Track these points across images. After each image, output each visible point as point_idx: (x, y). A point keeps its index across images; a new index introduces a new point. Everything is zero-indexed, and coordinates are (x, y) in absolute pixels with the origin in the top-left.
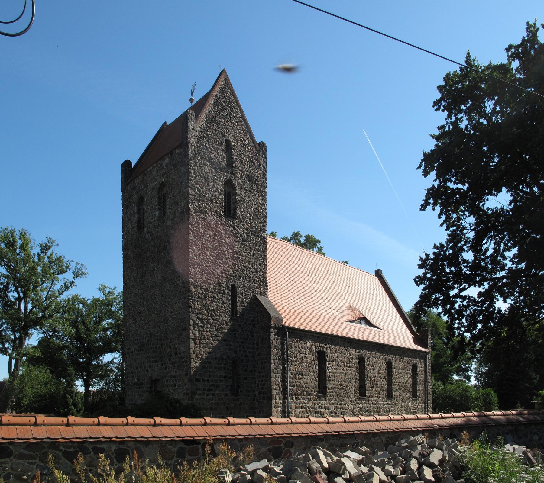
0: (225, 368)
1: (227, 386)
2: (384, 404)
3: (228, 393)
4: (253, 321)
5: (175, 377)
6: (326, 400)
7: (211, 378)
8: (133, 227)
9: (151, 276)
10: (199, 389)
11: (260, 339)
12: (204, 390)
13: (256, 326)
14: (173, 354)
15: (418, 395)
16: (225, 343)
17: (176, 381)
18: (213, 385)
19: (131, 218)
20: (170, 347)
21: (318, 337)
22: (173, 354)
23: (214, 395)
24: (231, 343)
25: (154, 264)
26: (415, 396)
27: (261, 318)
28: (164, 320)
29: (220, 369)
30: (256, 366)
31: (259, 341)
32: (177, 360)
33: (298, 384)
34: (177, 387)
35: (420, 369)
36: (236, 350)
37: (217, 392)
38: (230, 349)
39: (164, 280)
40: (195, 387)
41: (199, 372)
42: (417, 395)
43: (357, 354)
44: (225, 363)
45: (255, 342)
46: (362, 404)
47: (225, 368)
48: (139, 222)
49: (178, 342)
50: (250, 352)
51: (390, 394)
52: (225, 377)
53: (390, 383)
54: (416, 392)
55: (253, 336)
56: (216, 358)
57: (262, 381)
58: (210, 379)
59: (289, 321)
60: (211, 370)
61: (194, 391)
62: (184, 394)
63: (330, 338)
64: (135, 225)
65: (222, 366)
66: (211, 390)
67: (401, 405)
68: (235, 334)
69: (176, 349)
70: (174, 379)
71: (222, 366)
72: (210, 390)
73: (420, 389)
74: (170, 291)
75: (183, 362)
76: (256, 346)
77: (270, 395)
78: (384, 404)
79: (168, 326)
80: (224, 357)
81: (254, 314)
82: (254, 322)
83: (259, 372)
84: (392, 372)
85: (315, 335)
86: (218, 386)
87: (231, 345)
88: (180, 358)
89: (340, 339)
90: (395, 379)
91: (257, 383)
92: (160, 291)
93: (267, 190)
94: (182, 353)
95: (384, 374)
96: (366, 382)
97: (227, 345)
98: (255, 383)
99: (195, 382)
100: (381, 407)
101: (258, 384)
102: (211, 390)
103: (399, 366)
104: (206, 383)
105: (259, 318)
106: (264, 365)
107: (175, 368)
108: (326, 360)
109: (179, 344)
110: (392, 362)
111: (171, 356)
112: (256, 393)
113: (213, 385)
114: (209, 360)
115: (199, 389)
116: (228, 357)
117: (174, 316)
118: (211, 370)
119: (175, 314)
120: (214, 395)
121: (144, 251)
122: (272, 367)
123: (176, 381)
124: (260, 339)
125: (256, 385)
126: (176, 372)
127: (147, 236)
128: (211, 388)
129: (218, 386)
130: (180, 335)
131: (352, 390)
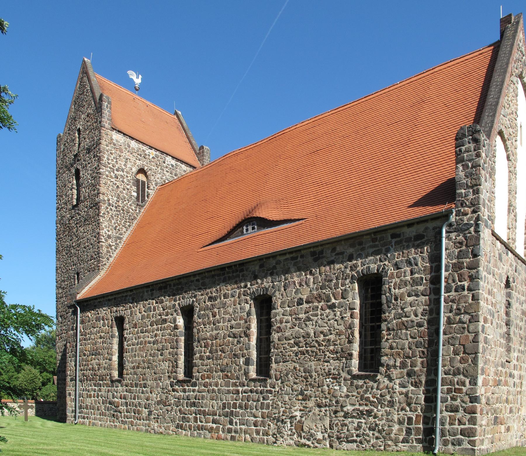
21: (115, 298)
46: (184, 391)
63: (130, 293)
85: (110, 298)
89: (145, 290)
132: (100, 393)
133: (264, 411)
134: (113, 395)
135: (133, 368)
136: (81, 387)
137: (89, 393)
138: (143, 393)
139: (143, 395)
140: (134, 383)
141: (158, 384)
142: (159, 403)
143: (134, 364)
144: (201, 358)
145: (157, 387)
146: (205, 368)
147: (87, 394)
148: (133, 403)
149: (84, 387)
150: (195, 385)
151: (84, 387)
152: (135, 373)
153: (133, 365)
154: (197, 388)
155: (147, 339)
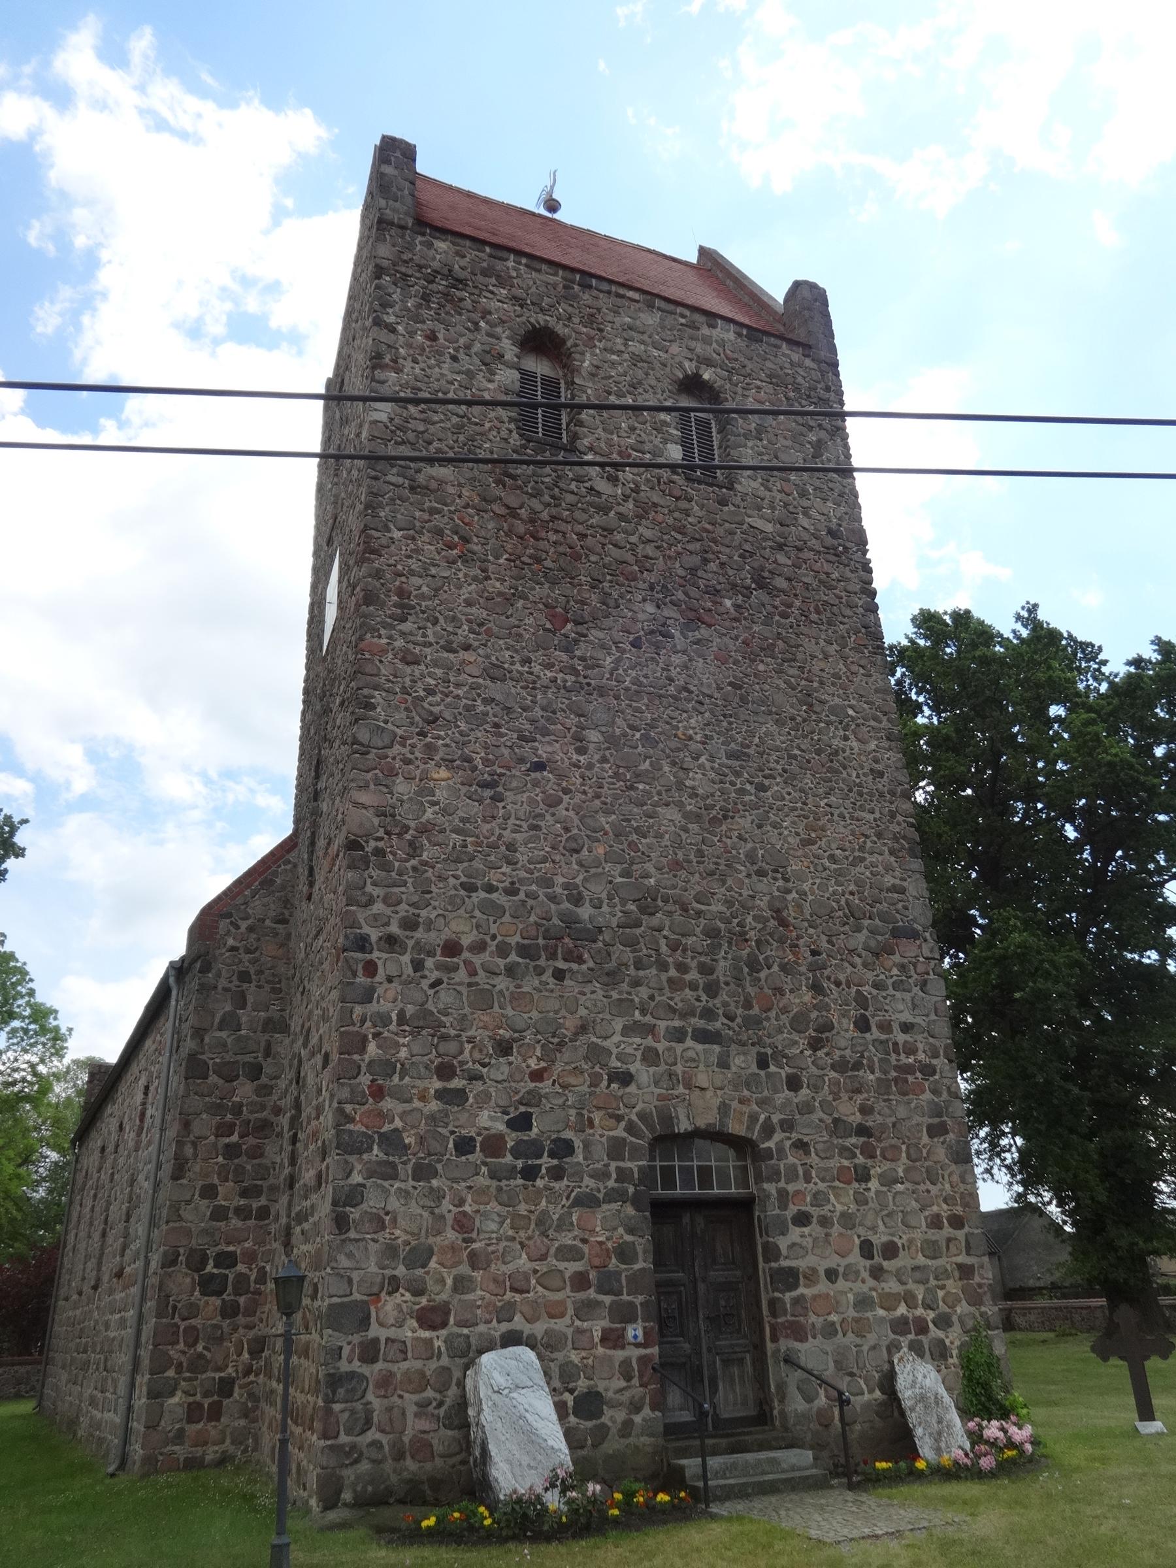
5: (862, 1131)
28: (751, 857)
34: (874, 1184)
62: (935, 1222)
69: (862, 1001)
75: (908, 1069)
109: (878, 986)
111: (828, 1027)
119: (832, 858)
126: (865, 1110)
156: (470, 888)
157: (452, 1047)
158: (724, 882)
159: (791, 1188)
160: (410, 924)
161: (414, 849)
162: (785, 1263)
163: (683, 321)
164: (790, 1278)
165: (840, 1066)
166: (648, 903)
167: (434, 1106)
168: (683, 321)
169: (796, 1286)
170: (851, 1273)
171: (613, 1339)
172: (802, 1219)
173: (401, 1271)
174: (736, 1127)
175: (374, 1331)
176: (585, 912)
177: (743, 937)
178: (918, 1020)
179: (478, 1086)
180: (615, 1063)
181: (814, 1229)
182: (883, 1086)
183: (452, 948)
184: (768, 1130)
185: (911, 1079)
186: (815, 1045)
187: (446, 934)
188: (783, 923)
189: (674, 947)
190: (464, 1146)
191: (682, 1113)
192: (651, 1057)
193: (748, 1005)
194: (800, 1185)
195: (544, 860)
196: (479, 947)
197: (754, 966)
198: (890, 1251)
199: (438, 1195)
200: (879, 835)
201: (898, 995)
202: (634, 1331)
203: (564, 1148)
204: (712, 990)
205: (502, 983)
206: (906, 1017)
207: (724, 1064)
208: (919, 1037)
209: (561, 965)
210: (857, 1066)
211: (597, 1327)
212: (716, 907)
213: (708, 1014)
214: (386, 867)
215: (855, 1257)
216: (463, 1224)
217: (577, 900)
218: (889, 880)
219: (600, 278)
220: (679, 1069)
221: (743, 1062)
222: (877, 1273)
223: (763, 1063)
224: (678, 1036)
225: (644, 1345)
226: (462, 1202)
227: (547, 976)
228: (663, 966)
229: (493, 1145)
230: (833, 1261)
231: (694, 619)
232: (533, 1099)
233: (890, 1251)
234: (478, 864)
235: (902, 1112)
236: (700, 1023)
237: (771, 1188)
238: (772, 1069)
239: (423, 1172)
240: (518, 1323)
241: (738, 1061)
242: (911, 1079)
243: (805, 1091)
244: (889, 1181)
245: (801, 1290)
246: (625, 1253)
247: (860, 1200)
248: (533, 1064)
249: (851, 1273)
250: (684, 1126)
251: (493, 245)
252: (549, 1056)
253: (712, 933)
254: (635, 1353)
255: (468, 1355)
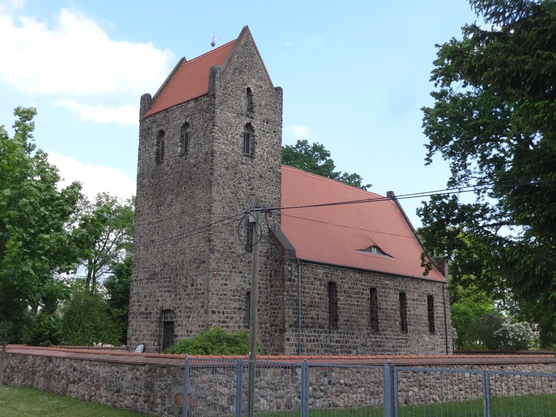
0: (239, 300)
1: (241, 318)
2: (398, 339)
3: (242, 324)
4: (267, 253)
5: (190, 308)
6: (337, 333)
7: (226, 310)
8: (151, 158)
9: (168, 207)
10: (214, 321)
11: (273, 271)
12: (219, 322)
13: (270, 258)
14: (189, 285)
15: (436, 329)
16: (241, 275)
17: (191, 312)
18: (227, 317)
19: (149, 149)
20: (186, 278)
22: (189, 285)
23: (227, 327)
24: (246, 275)
25: (173, 196)
26: (432, 330)
27: (275, 250)
28: (181, 251)
29: (235, 301)
30: (269, 298)
31: (273, 273)
32: (194, 291)
33: (310, 316)
34: (191, 319)
35: (438, 302)
36: (250, 281)
37: (230, 324)
38: (245, 281)
39: (184, 212)
40: (211, 319)
41: (215, 304)
42: (434, 329)
43: (369, 284)
44: (239, 294)
45: (268, 274)
46: (375, 338)
47: (239, 300)
48: (157, 153)
49: (195, 274)
50: (263, 284)
51: (404, 328)
52: (240, 309)
53: (403, 315)
54: (434, 326)
55: (266, 268)
56: (231, 291)
57: (274, 313)
58: (225, 311)
59: (301, 254)
60: (226, 302)
61: (210, 323)
62: (199, 326)
64: (153, 156)
65: (237, 297)
66: (226, 322)
67: (418, 341)
68: (250, 266)
70: (189, 310)
71: (237, 297)
72: (224, 322)
73: (438, 322)
74: (190, 224)
75: (199, 294)
76: (268, 277)
77: (282, 328)
78: (398, 339)
79: (185, 257)
80: (239, 289)
81: (268, 246)
82: (268, 254)
83: (272, 304)
84: (406, 303)
86: (232, 318)
87: (245, 277)
88: (197, 289)
90: (409, 311)
91: (269, 315)
92: (179, 223)
93: (283, 129)
94: (199, 285)
95: (397, 306)
96: (379, 314)
97: (242, 277)
98: (267, 315)
99: (211, 314)
100: (395, 342)
101: (270, 316)
102: (226, 322)
103: (414, 298)
104: (221, 314)
105: (273, 250)
106: (277, 297)
107: (190, 300)
108: (336, 291)
109: (196, 276)
110: (406, 292)
111: (187, 287)
112: (268, 325)
113: (227, 317)
114: (225, 293)
115: (214, 321)
116: (243, 289)
117: (193, 249)
118: (226, 302)
120: (227, 327)
121: (162, 182)
122: (285, 299)
123: (191, 313)
124: (273, 271)
125: (268, 317)
126: (191, 303)
127: (166, 169)
128: (226, 320)
129: (232, 318)
130: (198, 267)
131: (364, 322)
132: (319, 339)
133: (407, 349)
134: (331, 340)
135: (345, 321)
136: (301, 333)
137: (309, 339)
138: (352, 338)
139: (351, 340)
140: (345, 331)
141: (361, 333)
142: (362, 345)
143: (345, 318)
144: (382, 319)
145: (360, 335)
146: (384, 325)
147: (307, 339)
148: (346, 346)
149: (304, 333)
150: (379, 335)
151: (304, 333)
152: (346, 325)
153: (344, 319)
154: (381, 336)
155: (352, 303)
156: (143, 268)
157: (140, 297)
158: (175, 258)
159: (178, 320)
160: (137, 277)
161: (138, 262)
162: (175, 333)
163: (184, 107)
164: (176, 336)
165: (188, 295)
166: (165, 264)
167: (138, 307)
168: (184, 107)
169: (176, 338)
170: (185, 336)
171: (154, 345)
172: (179, 325)
173: (134, 333)
174: (171, 309)
175: (131, 341)
176: (156, 270)
177: (176, 270)
178: (203, 283)
179: (142, 304)
180: (157, 298)
181: (180, 327)
182: (195, 298)
183: (141, 280)
184: (175, 309)
185: (199, 296)
186: (185, 290)
187: (140, 278)
188: (183, 265)
189: (167, 274)
190: (141, 314)
191: (164, 306)
192: (161, 296)
193: (175, 284)
194: (179, 319)
195: (153, 260)
196: (144, 279)
197: (177, 275)
198: (191, 332)
199: (137, 321)
200: (202, 239)
201: (200, 277)
202: (156, 344)
203: (150, 313)
204: (170, 282)
205: (146, 285)
206: (201, 282)
207: (171, 297)
208: (202, 286)
209: (152, 281)
210: (190, 294)
211: (152, 342)
212: (174, 264)
213: (169, 287)
214: (135, 267)
215: (186, 333)
216: (140, 326)
217: (155, 267)
218: (203, 250)
219: (169, 108)
220: (165, 298)
221: (173, 296)
222: (188, 336)
223: (176, 296)
224: (165, 292)
225: (157, 346)
226: (140, 323)
227: (151, 283)
228: (164, 278)
229: (143, 313)
230: (183, 333)
231: (178, 195)
232: (148, 305)
233: (191, 332)
234: (145, 264)
235: (197, 303)
236: (167, 289)
237: (175, 319)
238: (177, 296)
239: (137, 318)
240: (144, 341)
241: (172, 296)
242: (199, 296)
243: (182, 300)
244: (194, 318)
245: (177, 338)
246: (156, 331)
247: (188, 322)
248: (148, 299)
249: (185, 336)
250: (164, 309)
251: (153, 114)
252: (150, 298)
253: (172, 270)
254: (156, 347)
255: (139, 344)
